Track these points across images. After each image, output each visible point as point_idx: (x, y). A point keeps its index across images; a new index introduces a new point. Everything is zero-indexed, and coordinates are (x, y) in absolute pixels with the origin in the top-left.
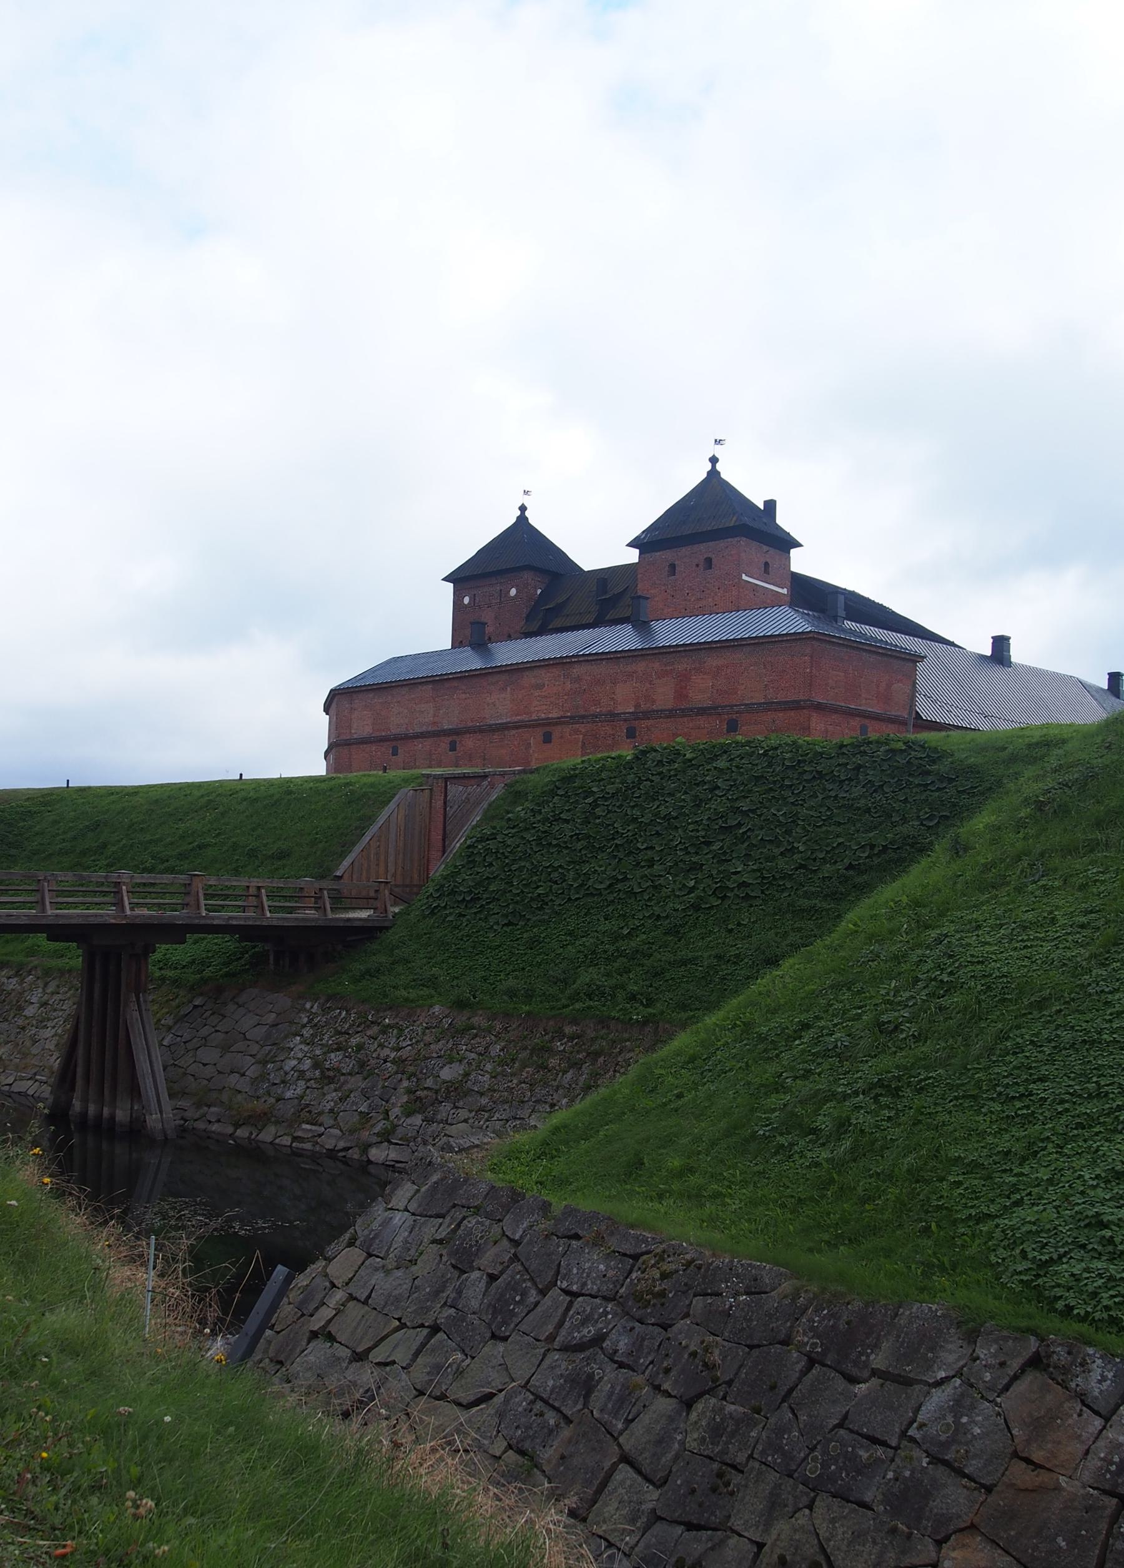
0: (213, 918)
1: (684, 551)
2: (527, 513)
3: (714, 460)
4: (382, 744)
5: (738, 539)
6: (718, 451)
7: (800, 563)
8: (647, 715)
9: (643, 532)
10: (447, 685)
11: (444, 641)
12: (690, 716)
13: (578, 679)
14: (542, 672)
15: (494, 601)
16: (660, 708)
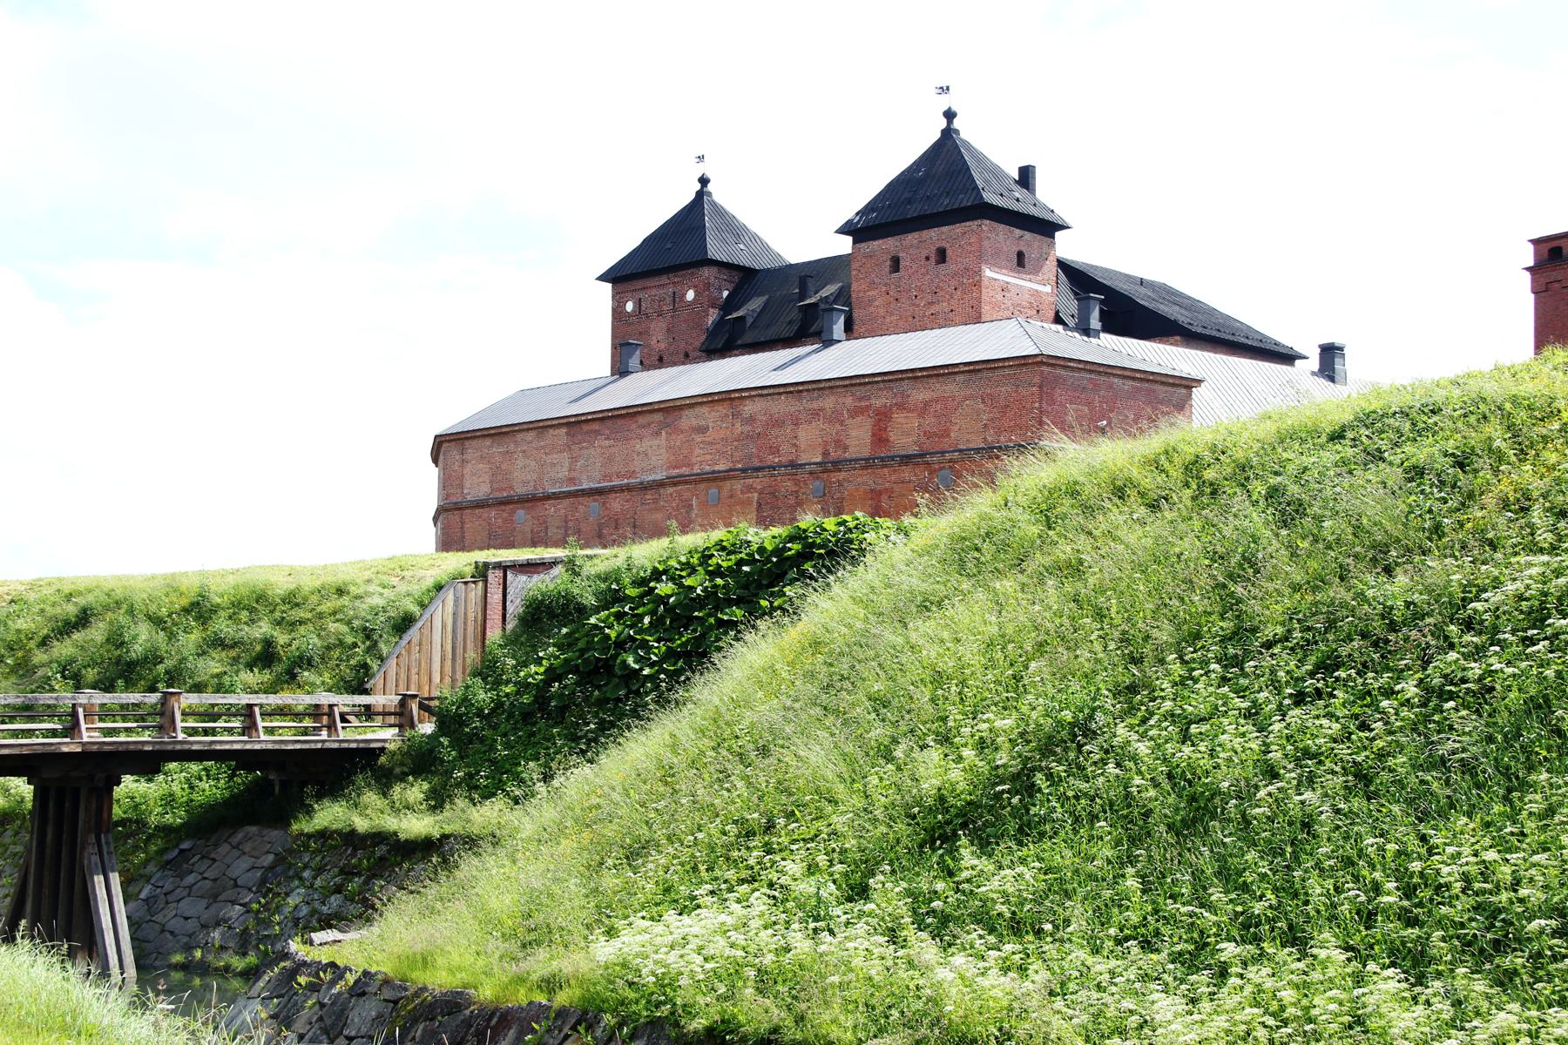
0: (192, 743)
1: (912, 238)
3: (950, 115)
4: (503, 507)
5: (979, 222)
7: (1066, 246)
8: (837, 465)
9: (857, 214)
10: (585, 427)
11: (600, 361)
13: (751, 420)
14: (705, 410)
15: (665, 308)
16: (854, 456)
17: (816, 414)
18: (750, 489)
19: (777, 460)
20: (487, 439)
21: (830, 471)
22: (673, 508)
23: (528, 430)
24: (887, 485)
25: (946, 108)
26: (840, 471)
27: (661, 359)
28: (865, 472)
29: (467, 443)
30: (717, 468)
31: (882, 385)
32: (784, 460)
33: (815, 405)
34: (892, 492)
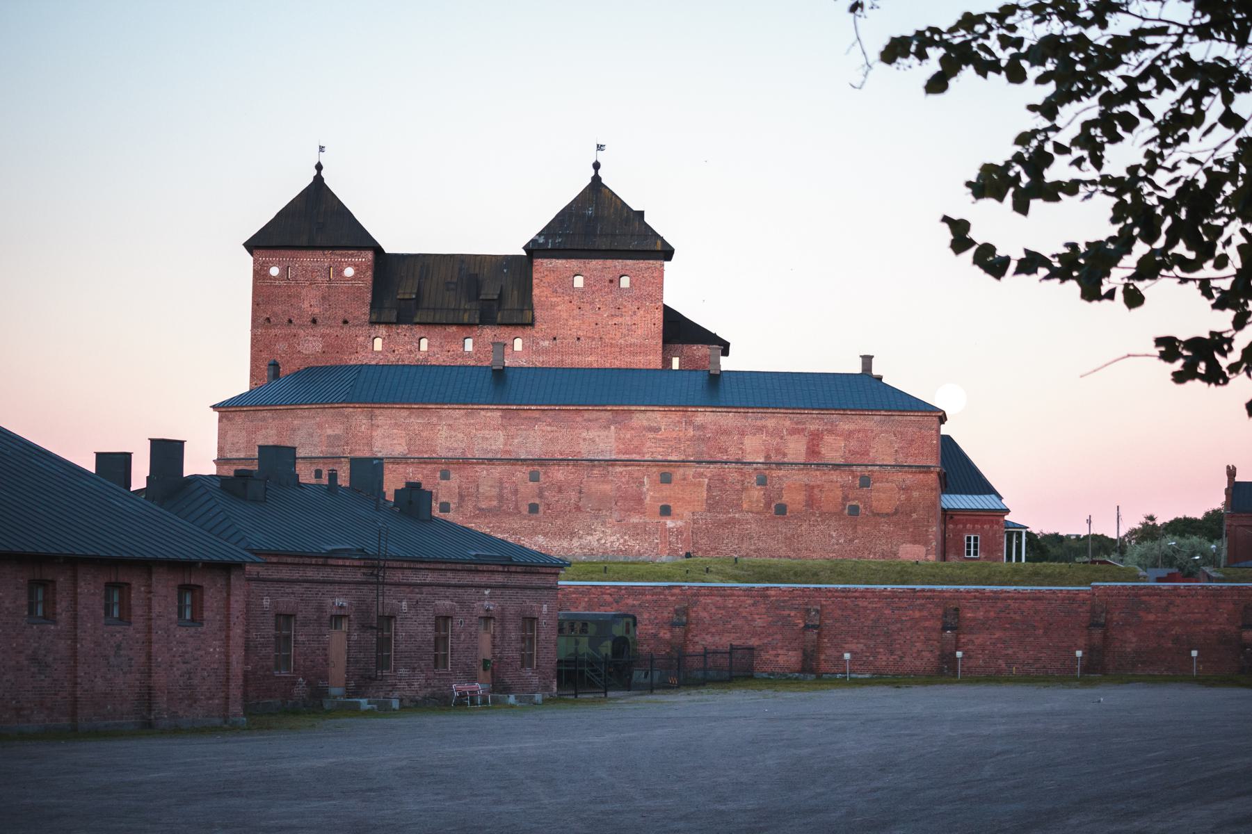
2: (323, 173)
4: (424, 466)
6: (602, 157)
8: (779, 465)
9: (539, 234)
12: (824, 470)
13: (702, 427)
16: (791, 461)
17: (760, 429)
18: (701, 475)
19: (725, 458)
20: (402, 411)
21: (772, 469)
22: (623, 483)
24: (819, 483)
25: (594, 161)
26: (781, 469)
28: (801, 472)
30: (669, 458)
31: (815, 416)
32: (732, 458)
33: (759, 423)
34: (823, 487)
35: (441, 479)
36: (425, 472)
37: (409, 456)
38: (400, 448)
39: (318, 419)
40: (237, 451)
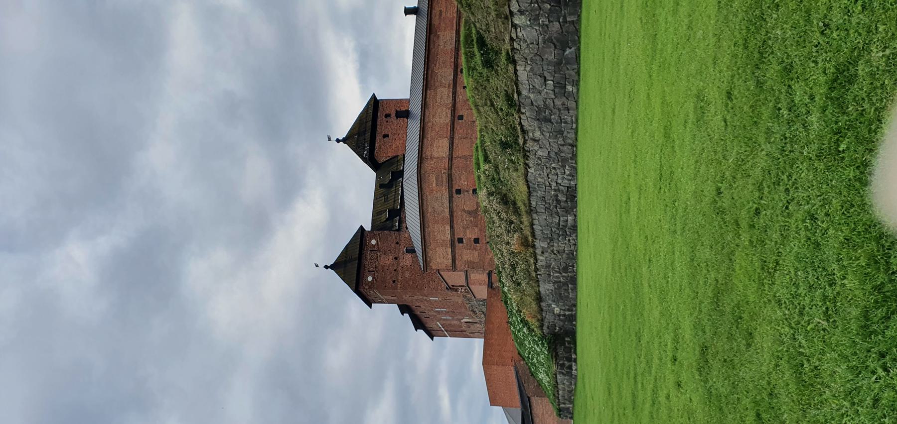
4: (455, 130)
14: (434, 11)
20: (424, 142)
23: (424, 114)
27: (396, 258)
29: (424, 155)
35: (463, 119)
36: (458, 128)
37: (449, 137)
38: (445, 143)
39: (427, 193)
40: (448, 254)
